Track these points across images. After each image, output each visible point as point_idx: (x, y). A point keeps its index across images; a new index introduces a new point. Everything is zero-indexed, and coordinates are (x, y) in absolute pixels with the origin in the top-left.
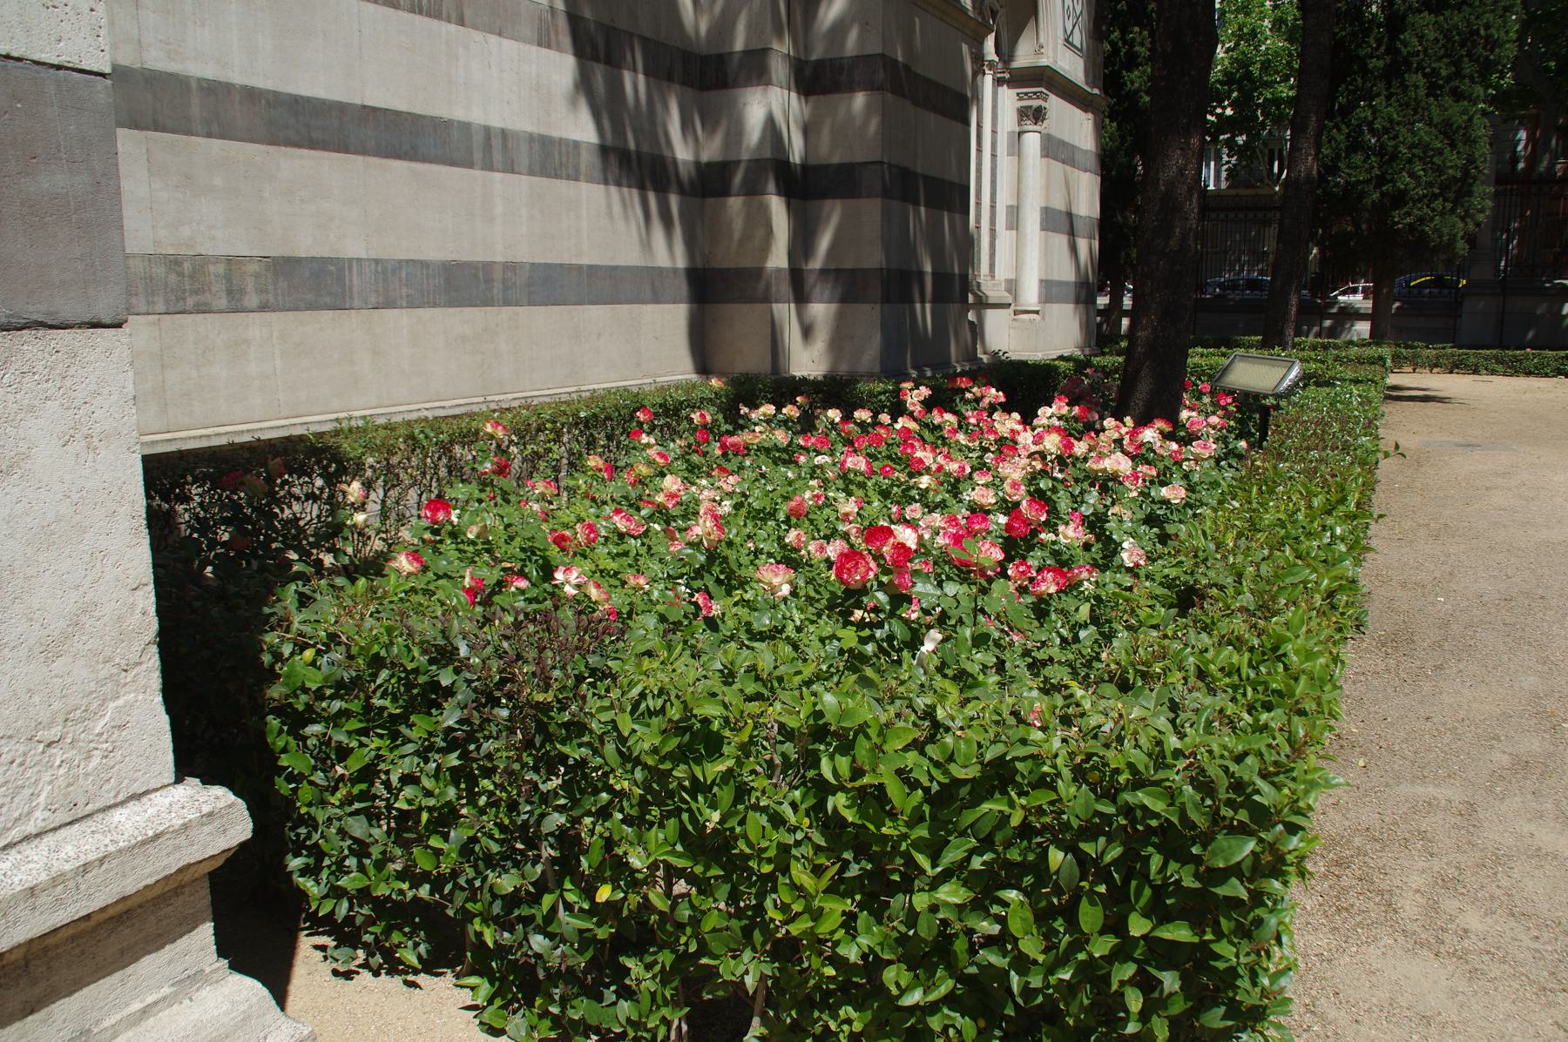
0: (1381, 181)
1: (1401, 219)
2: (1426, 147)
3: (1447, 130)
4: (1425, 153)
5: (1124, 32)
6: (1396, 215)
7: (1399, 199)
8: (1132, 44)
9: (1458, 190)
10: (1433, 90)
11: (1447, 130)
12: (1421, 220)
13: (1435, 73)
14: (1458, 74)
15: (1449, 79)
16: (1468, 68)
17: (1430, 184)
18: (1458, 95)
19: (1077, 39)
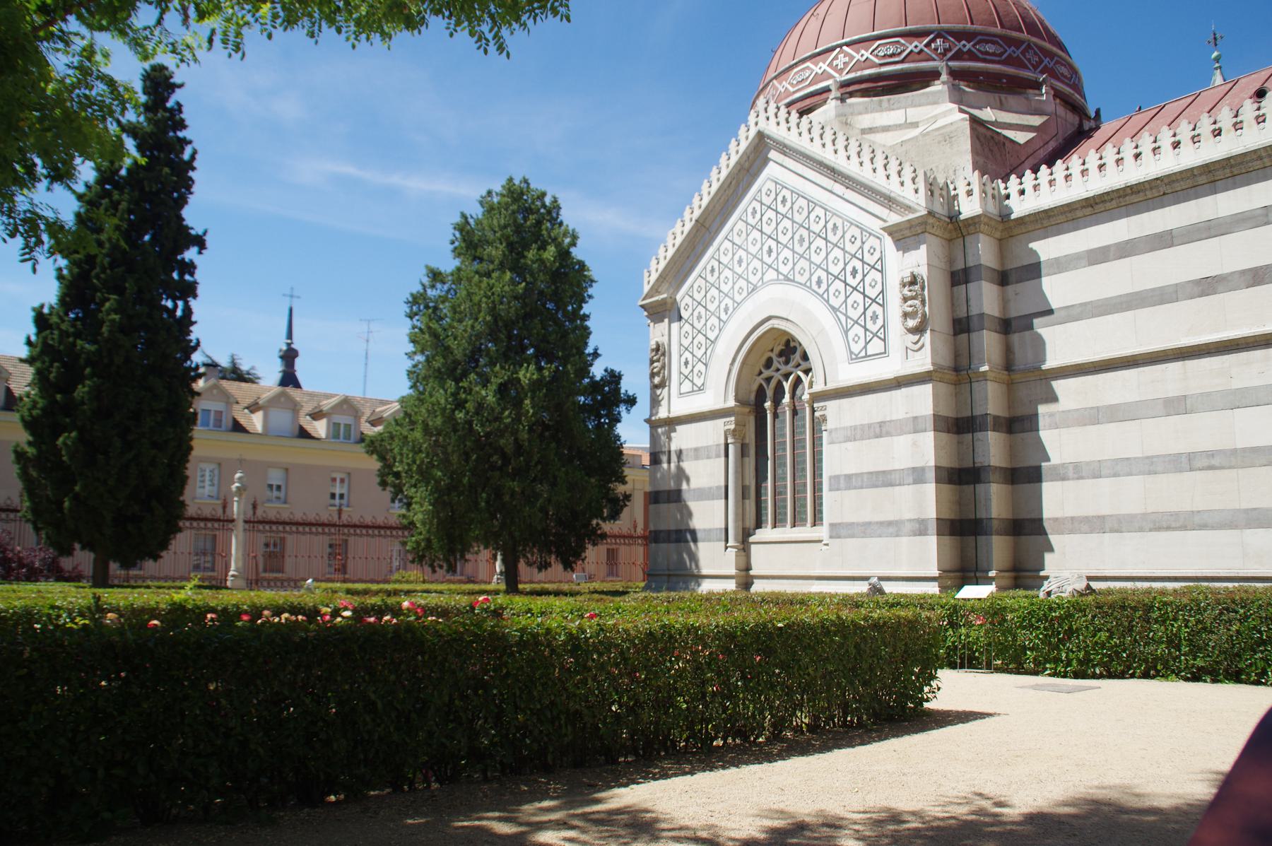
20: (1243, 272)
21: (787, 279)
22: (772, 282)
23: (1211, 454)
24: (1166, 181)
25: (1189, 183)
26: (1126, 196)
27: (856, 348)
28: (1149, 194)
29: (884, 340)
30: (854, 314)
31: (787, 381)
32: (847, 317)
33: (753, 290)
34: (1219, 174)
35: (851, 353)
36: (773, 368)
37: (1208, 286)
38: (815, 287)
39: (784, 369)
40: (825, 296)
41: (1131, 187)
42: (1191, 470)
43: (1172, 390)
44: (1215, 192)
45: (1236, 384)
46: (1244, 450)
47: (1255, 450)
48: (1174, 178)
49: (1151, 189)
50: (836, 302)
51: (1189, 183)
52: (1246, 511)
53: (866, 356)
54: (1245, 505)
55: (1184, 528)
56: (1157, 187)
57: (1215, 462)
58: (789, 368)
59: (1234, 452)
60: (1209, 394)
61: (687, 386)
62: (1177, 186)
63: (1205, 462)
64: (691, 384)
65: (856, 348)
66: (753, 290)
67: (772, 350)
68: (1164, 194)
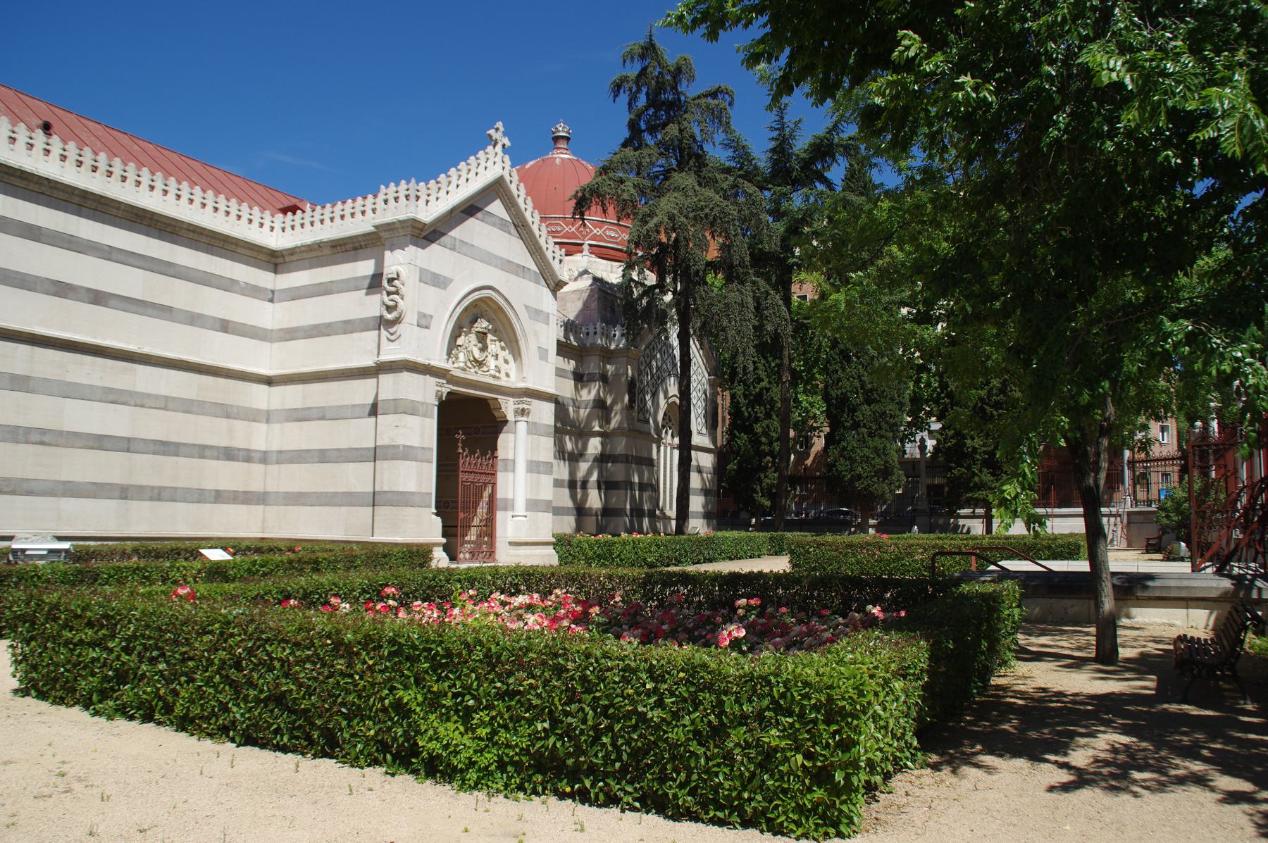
0: (851, 470)
1: (859, 485)
2: (868, 458)
3: (876, 450)
4: (867, 459)
5: (753, 409)
6: (857, 484)
7: (859, 477)
8: (756, 413)
9: (885, 473)
10: (870, 435)
11: (876, 450)
12: (868, 485)
13: (870, 428)
14: (880, 428)
15: (876, 430)
16: (884, 425)
17: (870, 472)
18: (881, 437)
19: (704, 431)
20: (89, 290)
23: (44, 432)
24: (52, 185)
25: (66, 196)
26: (14, 176)
28: (32, 186)
34: (89, 203)
37: (62, 290)
41: (22, 172)
42: (27, 442)
43: (19, 369)
44: (79, 214)
45: (70, 378)
46: (68, 433)
47: (76, 434)
48: (59, 186)
49: (36, 183)
51: (66, 196)
52: (65, 483)
54: (64, 478)
55: (13, 493)
56: (41, 184)
57: (47, 439)
59: (61, 433)
60: (49, 380)
62: (56, 194)
63: (37, 437)
68: (43, 193)
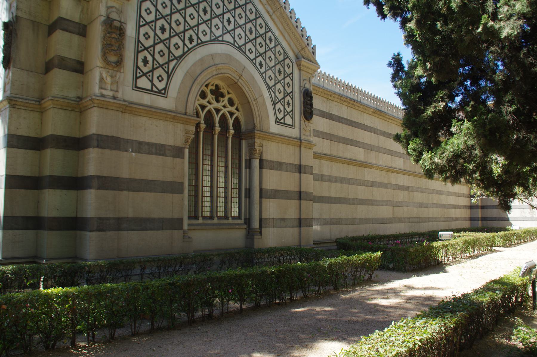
21: (239, 48)
22: (228, 43)
27: (280, 116)
29: (293, 119)
30: (280, 96)
31: (203, 110)
32: (275, 96)
33: (214, 40)
35: (277, 118)
36: (207, 100)
38: (259, 67)
39: (216, 105)
40: (264, 75)
50: (271, 83)
53: (284, 123)
58: (219, 106)
61: (144, 83)
64: (150, 84)
65: (280, 116)
66: (214, 40)
67: (207, 86)
